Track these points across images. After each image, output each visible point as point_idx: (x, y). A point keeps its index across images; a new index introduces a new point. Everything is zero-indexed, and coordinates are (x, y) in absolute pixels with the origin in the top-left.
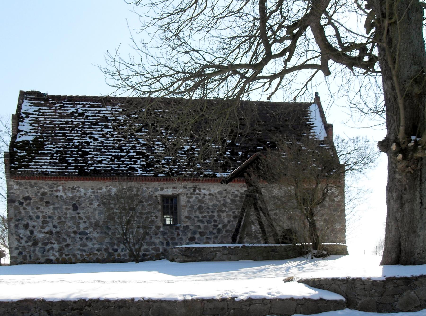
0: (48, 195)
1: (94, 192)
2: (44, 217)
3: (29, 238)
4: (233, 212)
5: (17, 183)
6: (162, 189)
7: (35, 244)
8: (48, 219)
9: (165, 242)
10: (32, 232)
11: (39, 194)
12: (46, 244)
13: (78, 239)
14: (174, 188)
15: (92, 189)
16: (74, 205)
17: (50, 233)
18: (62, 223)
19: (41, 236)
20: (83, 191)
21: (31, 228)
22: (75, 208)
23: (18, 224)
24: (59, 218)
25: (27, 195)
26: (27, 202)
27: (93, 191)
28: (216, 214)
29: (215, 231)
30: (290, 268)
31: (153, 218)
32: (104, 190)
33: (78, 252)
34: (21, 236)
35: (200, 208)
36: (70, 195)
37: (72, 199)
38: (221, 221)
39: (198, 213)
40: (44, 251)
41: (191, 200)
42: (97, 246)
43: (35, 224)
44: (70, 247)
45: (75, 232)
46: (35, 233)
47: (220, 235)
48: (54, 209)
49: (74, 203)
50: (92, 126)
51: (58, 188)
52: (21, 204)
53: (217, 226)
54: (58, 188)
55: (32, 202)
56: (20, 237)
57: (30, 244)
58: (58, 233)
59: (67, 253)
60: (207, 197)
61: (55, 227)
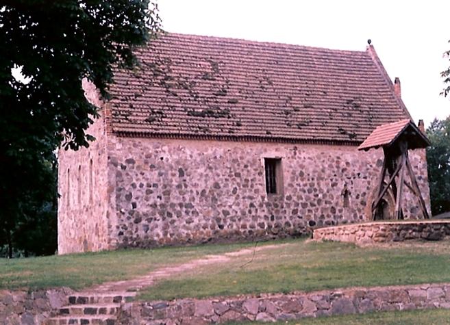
0: (153, 156)
1: (199, 155)
2: (149, 186)
3: (131, 213)
4: (332, 180)
5: (120, 141)
6: (266, 151)
7: (138, 221)
8: (152, 188)
9: (270, 216)
10: (134, 205)
11: (144, 157)
12: (149, 220)
13: (183, 213)
14: (276, 150)
15: (198, 150)
16: (180, 171)
17: (154, 206)
18: (167, 193)
19: (145, 210)
20: (188, 152)
21: (133, 200)
22: (181, 173)
23: (120, 195)
24: (165, 186)
25: (130, 157)
26: (131, 165)
27: (199, 152)
28: (315, 182)
29: (316, 203)
30: (397, 173)
31: (258, 186)
32: (210, 152)
33: (183, 230)
34: (123, 210)
35: (302, 174)
36: (175, 157)
37: (178, 162)
38: (321, 191)
39: (299, 181)
40: (148, 229)
41: (292, 165)
42: (203, 222)
43: (139, 194)
44: (176, 224)
45: (181, 205)
46: (138, 206)
47: (321, 206)
48: (160, 174)
49: (180, 167)
50: (358, 122)
51: (164, 148)
52: (124, 168)
53: (318, 195)
54: (164, 148)
55: (136, 165)
56: (121, 212)
57: (132, 220)
58: (162, 205)
59: (172, 232)
60: (308, 161)
61: (160, 197)
